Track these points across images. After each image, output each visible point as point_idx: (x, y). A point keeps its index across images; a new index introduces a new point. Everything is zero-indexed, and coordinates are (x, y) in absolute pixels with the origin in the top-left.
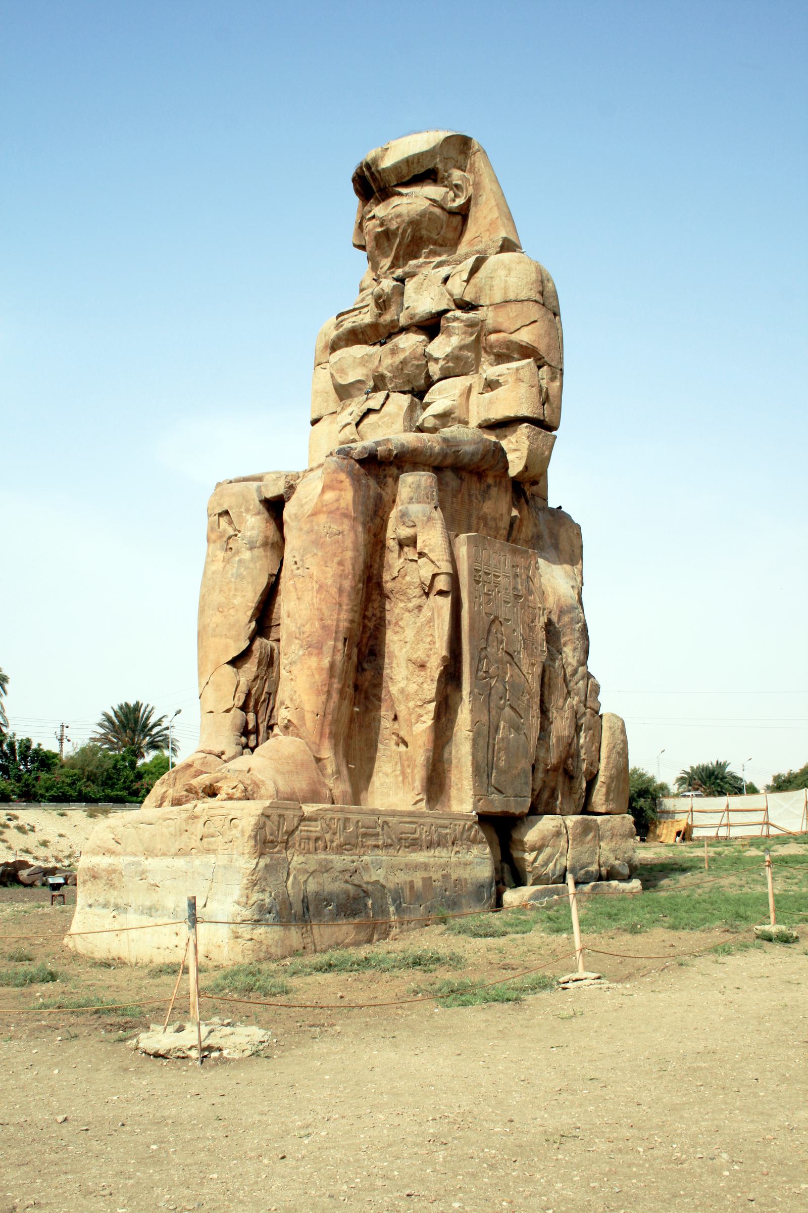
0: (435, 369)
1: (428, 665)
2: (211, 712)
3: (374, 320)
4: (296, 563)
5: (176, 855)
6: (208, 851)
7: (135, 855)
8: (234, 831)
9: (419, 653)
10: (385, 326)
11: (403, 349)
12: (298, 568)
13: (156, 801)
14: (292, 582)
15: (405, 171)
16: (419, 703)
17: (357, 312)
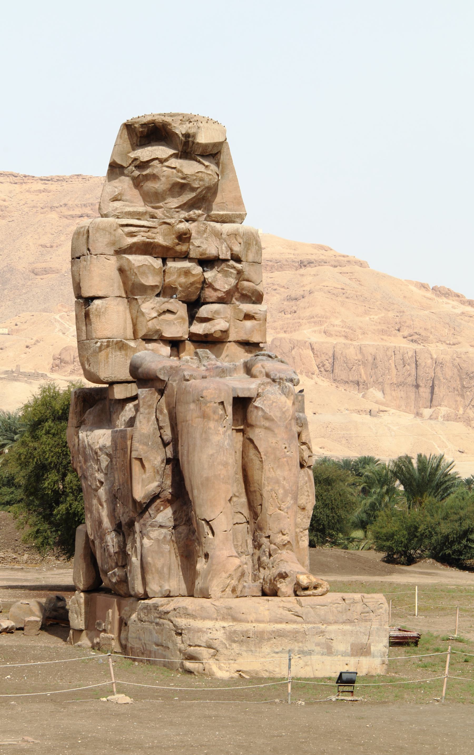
0: (209, 294)
1: (307, 508)
2: (226, 531)
3: (172, 246)
4: (285, 448)
5: (344, 622)
6: (366, 621)
7: (315, 623)
8: (381, 610)
9: (302, 501)
10: (176, 252)
11: (193, 275)
12: (288, 452)
13: (222, 588)
14: (285, 459)
15: (209, 150)
16: (302, 530)
17: (148, 229)
